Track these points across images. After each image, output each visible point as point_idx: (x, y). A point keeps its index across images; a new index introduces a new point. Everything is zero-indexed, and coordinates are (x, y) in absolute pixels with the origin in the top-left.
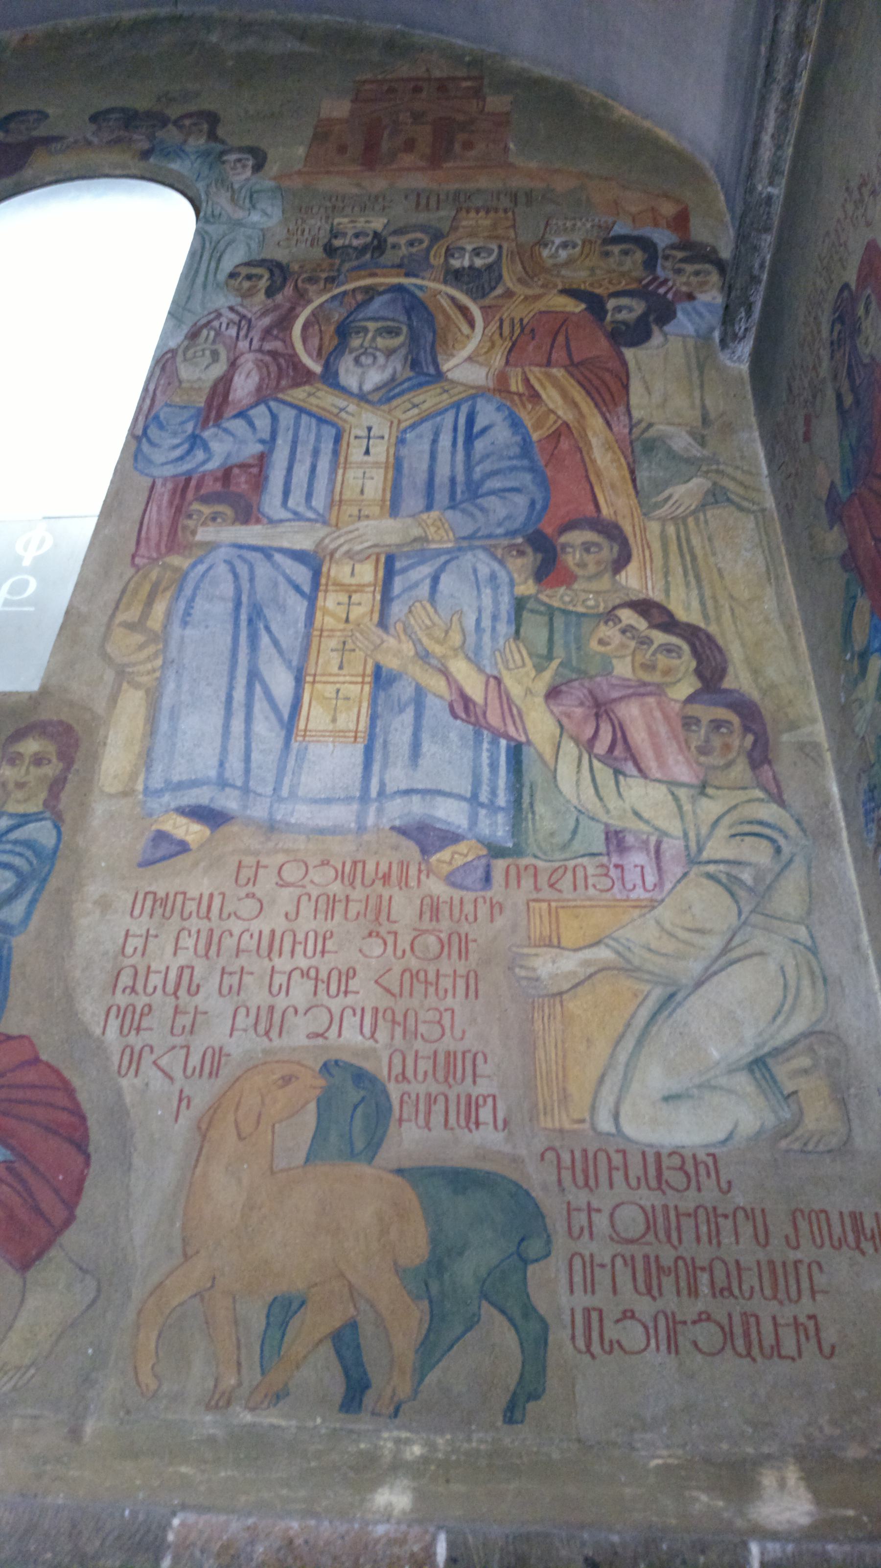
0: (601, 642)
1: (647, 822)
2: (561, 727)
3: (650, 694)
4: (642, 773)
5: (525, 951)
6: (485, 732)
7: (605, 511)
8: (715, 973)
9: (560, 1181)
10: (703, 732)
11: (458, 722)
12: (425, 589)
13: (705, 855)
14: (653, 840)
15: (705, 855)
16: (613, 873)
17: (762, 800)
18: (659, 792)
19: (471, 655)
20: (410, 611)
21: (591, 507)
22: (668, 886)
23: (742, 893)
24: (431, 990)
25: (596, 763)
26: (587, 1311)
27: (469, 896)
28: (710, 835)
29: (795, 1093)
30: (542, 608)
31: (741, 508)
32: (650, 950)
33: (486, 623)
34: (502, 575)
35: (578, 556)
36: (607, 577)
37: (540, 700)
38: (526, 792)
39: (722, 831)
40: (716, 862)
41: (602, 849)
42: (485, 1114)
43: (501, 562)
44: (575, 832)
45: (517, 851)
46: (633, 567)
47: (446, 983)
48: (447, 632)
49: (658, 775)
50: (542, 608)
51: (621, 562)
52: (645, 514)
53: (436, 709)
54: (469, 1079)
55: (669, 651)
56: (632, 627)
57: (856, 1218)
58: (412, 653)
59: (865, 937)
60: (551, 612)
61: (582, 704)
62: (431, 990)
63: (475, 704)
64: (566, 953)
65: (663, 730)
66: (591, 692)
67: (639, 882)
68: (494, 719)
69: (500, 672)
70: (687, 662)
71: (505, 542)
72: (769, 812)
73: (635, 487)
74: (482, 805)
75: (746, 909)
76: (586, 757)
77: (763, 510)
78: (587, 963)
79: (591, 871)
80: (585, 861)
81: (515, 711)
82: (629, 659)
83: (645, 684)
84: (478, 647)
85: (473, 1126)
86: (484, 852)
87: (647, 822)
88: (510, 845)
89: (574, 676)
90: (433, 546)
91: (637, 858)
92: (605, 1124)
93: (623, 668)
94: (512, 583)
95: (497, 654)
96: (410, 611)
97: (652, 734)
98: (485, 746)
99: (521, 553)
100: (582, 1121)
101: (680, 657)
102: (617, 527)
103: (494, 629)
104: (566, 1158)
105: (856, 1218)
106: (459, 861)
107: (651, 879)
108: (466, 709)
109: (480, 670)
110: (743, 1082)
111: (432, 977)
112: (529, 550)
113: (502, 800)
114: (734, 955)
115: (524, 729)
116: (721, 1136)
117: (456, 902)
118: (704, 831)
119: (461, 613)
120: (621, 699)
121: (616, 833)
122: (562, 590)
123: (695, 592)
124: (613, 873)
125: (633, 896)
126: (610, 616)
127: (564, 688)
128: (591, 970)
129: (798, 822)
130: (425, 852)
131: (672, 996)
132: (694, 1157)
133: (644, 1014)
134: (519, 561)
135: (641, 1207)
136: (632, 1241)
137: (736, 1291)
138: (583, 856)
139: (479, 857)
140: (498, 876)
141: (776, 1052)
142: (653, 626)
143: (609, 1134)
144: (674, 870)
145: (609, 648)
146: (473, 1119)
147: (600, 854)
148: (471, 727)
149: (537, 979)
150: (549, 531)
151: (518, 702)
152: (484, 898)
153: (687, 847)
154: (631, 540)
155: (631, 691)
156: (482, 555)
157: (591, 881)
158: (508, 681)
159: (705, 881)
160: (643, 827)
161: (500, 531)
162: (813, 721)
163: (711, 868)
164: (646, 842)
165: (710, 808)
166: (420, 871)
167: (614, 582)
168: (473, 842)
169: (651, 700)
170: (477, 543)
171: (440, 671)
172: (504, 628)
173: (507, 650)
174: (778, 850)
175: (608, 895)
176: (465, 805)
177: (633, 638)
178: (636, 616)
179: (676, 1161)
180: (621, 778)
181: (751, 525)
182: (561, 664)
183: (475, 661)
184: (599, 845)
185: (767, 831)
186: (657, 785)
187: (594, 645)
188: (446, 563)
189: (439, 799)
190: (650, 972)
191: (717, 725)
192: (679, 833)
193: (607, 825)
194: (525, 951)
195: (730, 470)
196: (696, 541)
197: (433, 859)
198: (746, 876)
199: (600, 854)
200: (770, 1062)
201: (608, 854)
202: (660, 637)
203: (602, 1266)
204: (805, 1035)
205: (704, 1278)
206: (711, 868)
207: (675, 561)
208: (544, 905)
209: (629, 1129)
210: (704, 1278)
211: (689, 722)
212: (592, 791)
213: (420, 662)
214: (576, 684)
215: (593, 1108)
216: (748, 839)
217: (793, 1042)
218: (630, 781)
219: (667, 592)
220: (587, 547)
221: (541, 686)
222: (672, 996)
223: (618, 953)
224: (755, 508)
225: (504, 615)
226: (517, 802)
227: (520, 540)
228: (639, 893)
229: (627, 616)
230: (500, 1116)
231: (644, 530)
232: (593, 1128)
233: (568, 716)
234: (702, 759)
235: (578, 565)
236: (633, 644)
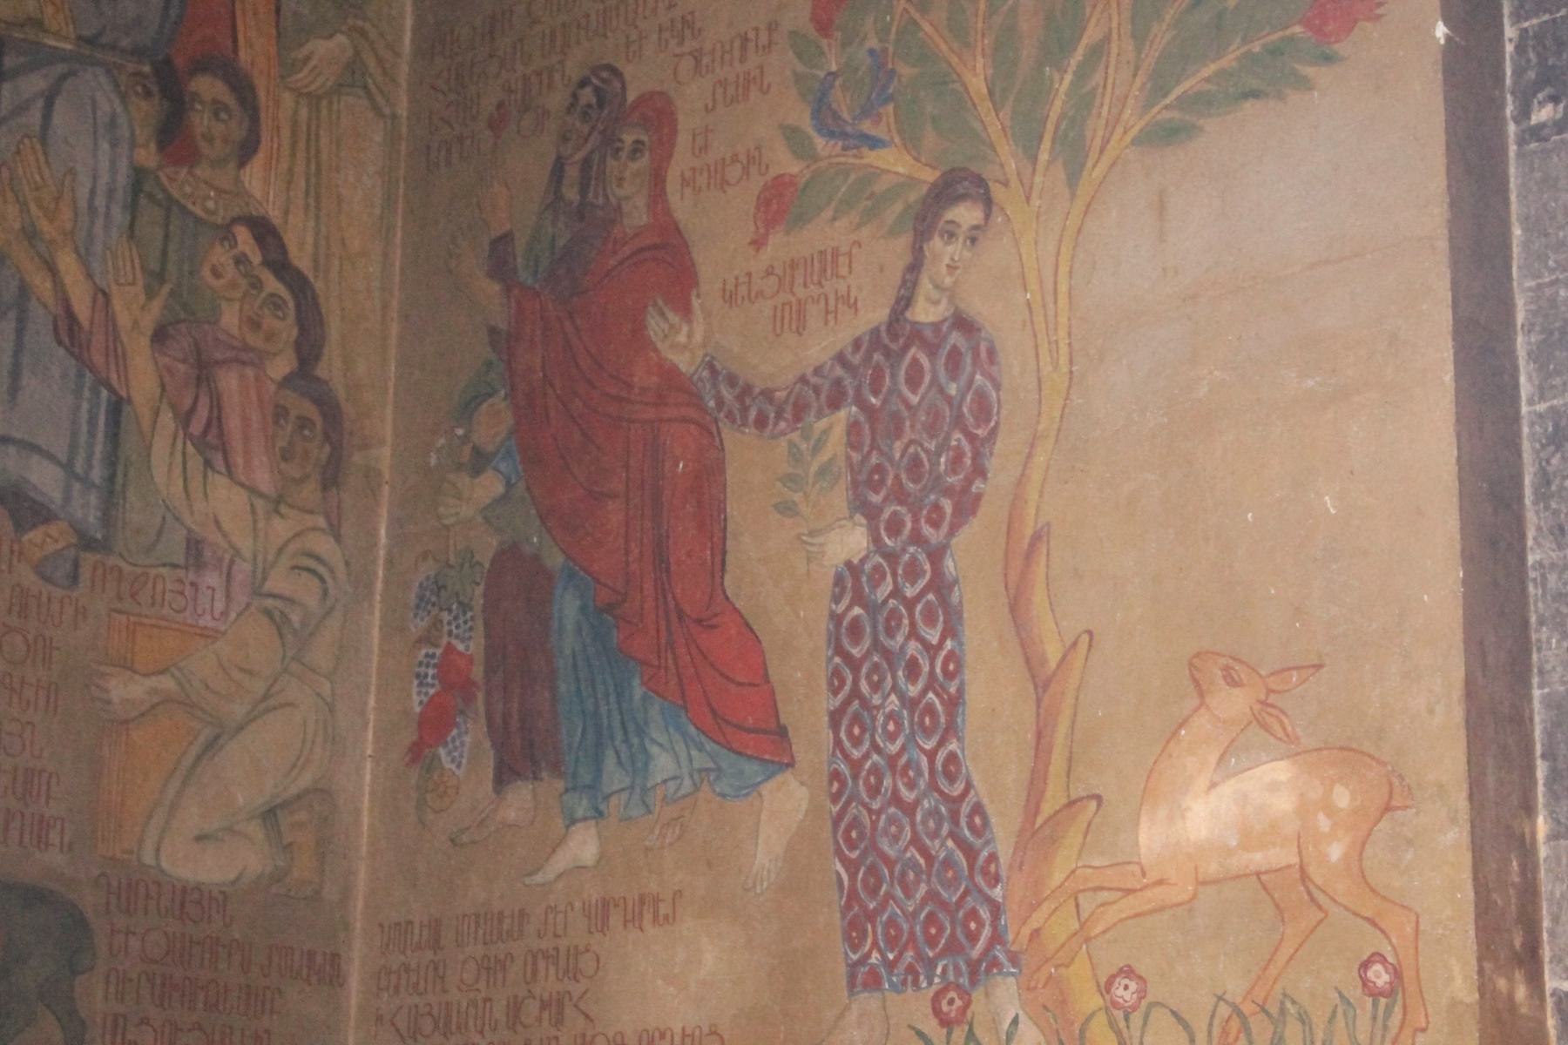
0: (216, 274)
1: (225, 535)
2: (163, 387)
3: (252, 363)
4: (230, 473)
5: (103, 668)
6: (88, 374)
7: (244, 56)
8: (252, 721)
9: (108, 903)
10: (290, 428)
11: (61, 351)
12: (35, 117)
13: (269, 586)
14: (227, 557)
15: (269, 586)
16: (188, 591)
17: (323, 530)
18: (239, 497)
19: (82, 251)
20: (18, 152)
21: (229, 43)
22: (233, 615)
23: (290, 637)
24: (15, 700)
25: (191, 449)
26: (116, 1016)
27: (58, 593)
28: (274, 564)
29: (290, 844)
30: (160, 196)
31: (376, 109)
32: (207, 687)
33: (100, 201)
34: (122, 120)
35: (206, 122)
36: (232, 165)
37: (145, 342)
38: (120, 469)
39: (285, 562)
40: (274, 596)
41: (182, 561)
42: (54, 837)
43: (124, 98)
44: (160, 533)
45: (104, 546)
46: (258, 161)
47: (29, 693)
48: (58, 199)
49: (243, 478)
50: (160, 196)
51: (247, 150)
52: (282, 77)
53: (40, 322)
54: (43, 800)
55: (277, 307)
56: (244, 255)
57: (311, 955)
58: (17, 226)
59: (372, 702)
60: (169, 205)
61: (184, 361)
62: (15, 700)
63: (80, 327)
64: (137, 677)
65: (255, 417)
66: (196, 344)
67: (208, 607)
68: (98, 359)
69: (109, 286)
70: (287, 329)
71: (131, 67)
72: (324, 545)
73: (277, 25)
74: (78, 478)
75: (290, 654)
76: (181, 433)
77: (394, 117)
78: (153, 691)
79: (169, 586)
80: (164, 571)
81: (119, 350)
82: (237, 306)
83: (247, 348)
84: (90, 238)
85: (43, 846)
86: (74, 540)
87: (225, 535)
88: (99, 536)
89: (183, 316)
90: (51, 42)
91: (212, 579)
92: (148, 859)
93: (230, 318)
94: (133, 144)
95: (108, 252)
96: (18, 152)
97: (246, 421)
98: (87, 393)
99: (148, 94)
100: (131, 852)
101: (284, 319)
102: (252, 88)
103: (107, 215)
104: (115, 883)
105: (311, 955)
106: (51, 548)
107: (219, 606)
108: (71, 329)
109: (89, 276)
110: (255, 830)
111: (17, 686)
112: (155, 89)
113: (97, 474)
114: (272, 702)
115: (127, 379)
116: (232, 877)
117: (44, 599)
118: (270, 558)
119: (72, 172)
120: (224, 362)
121: (198, 542)
122: (184, 172)
123: (312, 224)
124: (188, 591)
125: (202, 623)
126: (226, 233)
127: (171, 330)
128: (155, 700)
129: (347, 564)
130: (20, 527)
131: (217, 737)
132: (210, 892)
133: (194, 751)
134: (144, 104)
135: (165, 933)
136: (156, 962)
137: (221, 1008)
138: (164, 565)
139: (68, 546)
140: (85, 573)
141: (285, 805)
142: (267, 263)
143: (150, 866)
144: (240, 598)
145: (222, 281)
146: (44, 840)
147: (175, 566)
148: (74, 362)
149: (109, 702)
150: (180, 62)
151: (125, 339)
152: (69, 597)
153: (254, 572)
154: (263, 115)
155: (229, 354)
156: (103, 79)
157: (168, 596)
158: (117, 304)
159: (265, 620)
160: (219, 539)
161: (125, 43)
162: (382, 442)
163: (269, 603)
164: (221, 560)
165: (281, 528)
166: (12, 552)
167: (238, 180)
168: (63, 525)
169: (250, 372)
170: (99, 55)
171: (46, 262)
172: (119, 216)
173: (119, 253)
174: (325, 593)
175: (180, 617)
176: (58, 473)
177: (245, 276)
178: (252, 241)
179: (196, 896)
180: (210, 473)
181: (378, 138)
182: (172, 293)
183: (84, 261)
184: (179, 558)
185: (321, 570)
186: (242, 491)
187: (206, 272)
188: (64, 77)
189: (35, 458)
190: (202, 710)
191: (304, 423)
192: (247, 553)
193: (189, 530)
194: (103, 668)
195: (373, 34)
196: (324, 141)
197: (25, 538)
198: (295, 618)
199: (175, 566)
200: (279, 812)
201: (187, 568)
202: (272, 284)
203: (131, 980)
204: (307, 791)
205: (201, 996)
206: (269, 602)
207: (300, 168)
208: (123, 618)
209: (164, 864)
210: (201, 996)
211: (280, 413)
212: (180, 483)
213: (26, 243)
214: (183, 327)
215: (141, 842)
216: (305, 574)
217: (299, 797)
218: (217, 476)
219: (286, 212)
220: (218, 108)
221: (148, 322)
222: (217, 737)
223: (180, 684)
224: (387, 111)
225: (120, 194)
226: (111, 479)
227: (147, 69)
228: (206, 621)
229: (243, 234)
230: (66, 839)
231: (277, 103)
232: (139, 860)
233: (169, 370)
234: (283, 466)
235: (203, 135)
236: (243, 282)
